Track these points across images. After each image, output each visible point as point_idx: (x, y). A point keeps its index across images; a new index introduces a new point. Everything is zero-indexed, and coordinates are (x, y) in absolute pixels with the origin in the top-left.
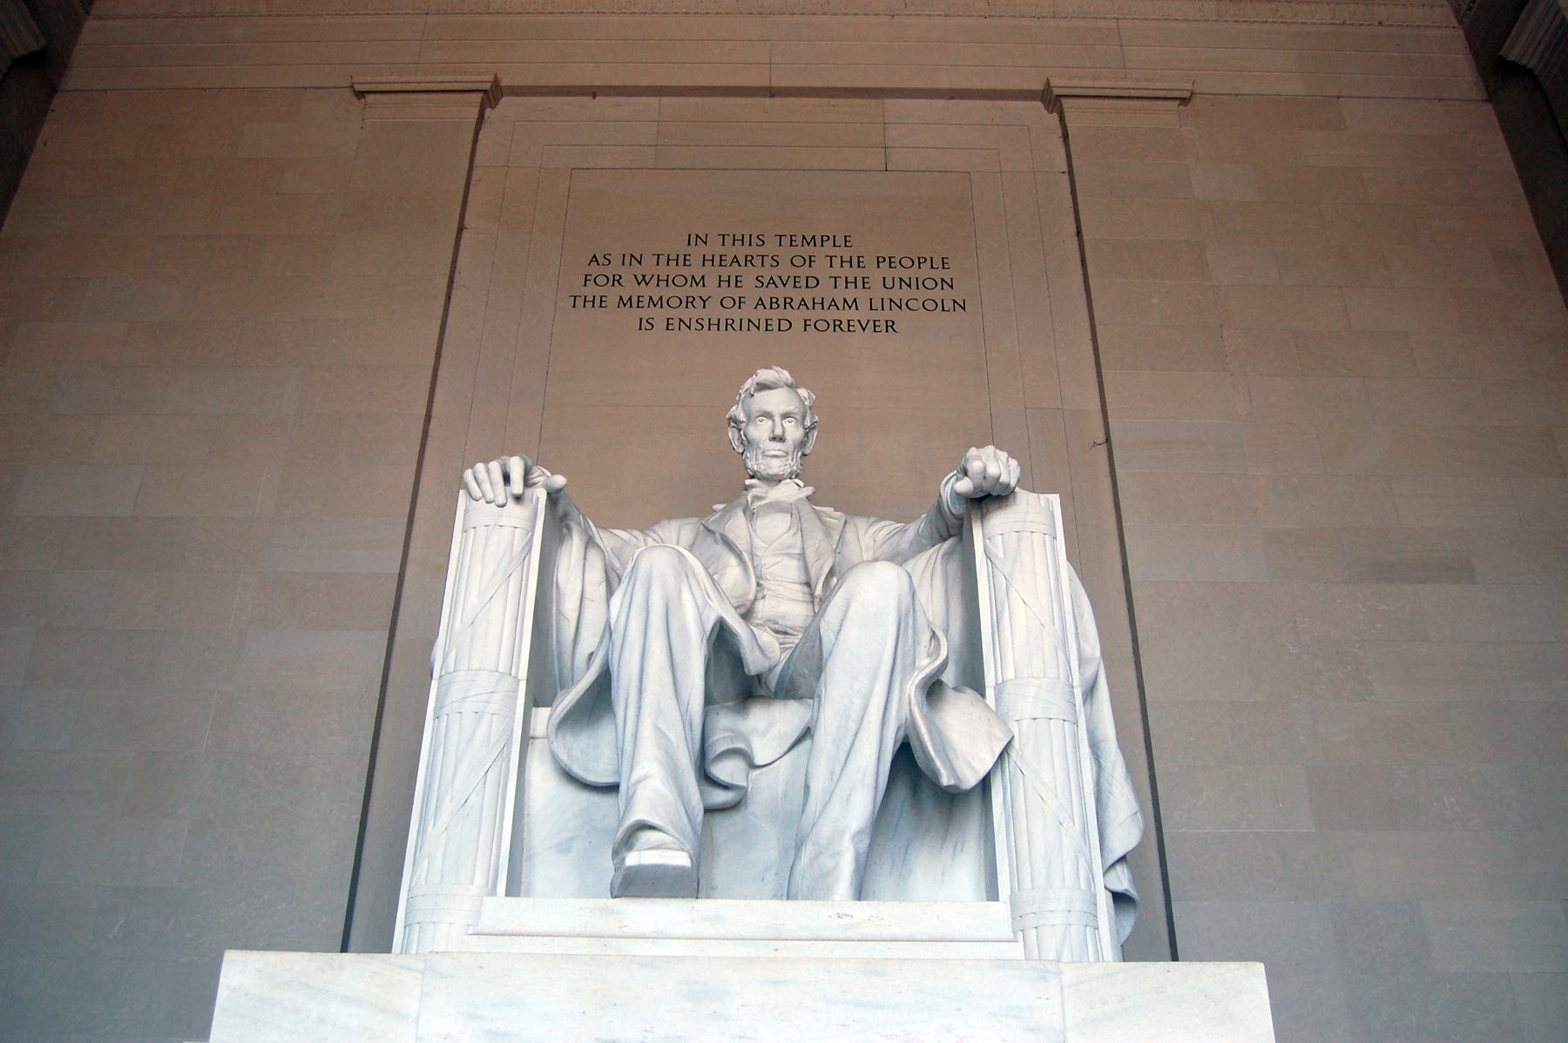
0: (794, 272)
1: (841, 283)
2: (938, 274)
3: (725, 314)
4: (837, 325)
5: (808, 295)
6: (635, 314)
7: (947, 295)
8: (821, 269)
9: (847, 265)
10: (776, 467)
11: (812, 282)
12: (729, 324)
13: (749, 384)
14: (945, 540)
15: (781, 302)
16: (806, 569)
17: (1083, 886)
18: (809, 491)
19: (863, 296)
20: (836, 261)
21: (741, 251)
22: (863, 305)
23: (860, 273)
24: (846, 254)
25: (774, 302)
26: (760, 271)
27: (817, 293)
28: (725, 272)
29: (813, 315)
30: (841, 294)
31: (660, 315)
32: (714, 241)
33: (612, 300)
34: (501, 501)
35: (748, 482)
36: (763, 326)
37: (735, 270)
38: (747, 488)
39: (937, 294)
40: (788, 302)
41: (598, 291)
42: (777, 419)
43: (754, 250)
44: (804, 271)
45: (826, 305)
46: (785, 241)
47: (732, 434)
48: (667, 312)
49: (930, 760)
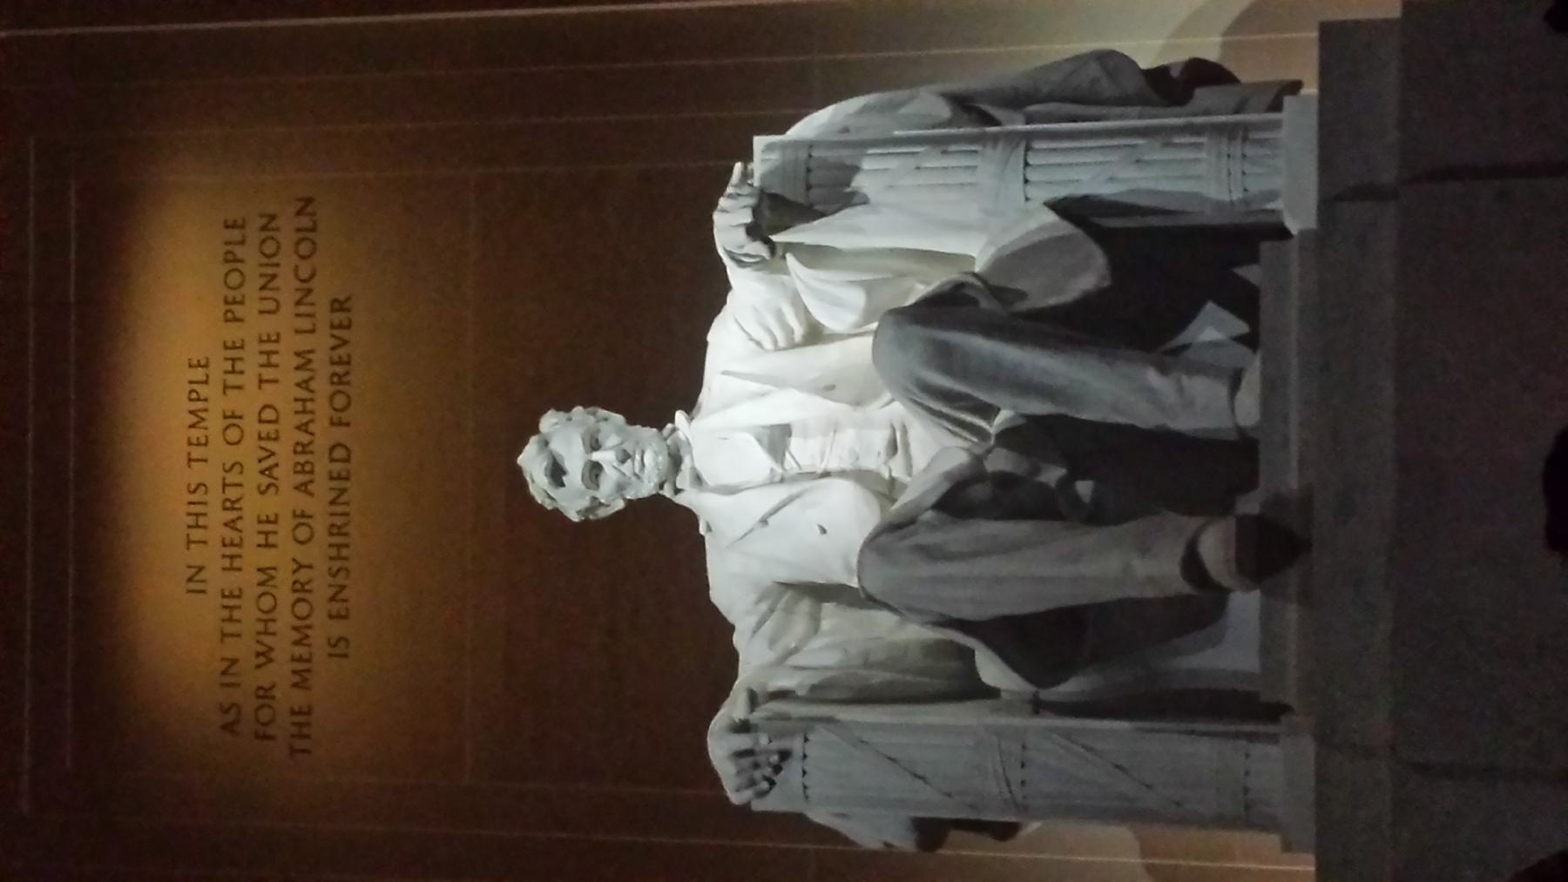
0: (251, 441)
1: (268, 373)
2: (253, 234)
5: (289, 420)
9: (239, 366)
10: (652, 460)
11: (269, 414)
15: (302, 459)
17: (1203, 140)
18: (680, 416)
20: (233, 380)
21: (216, 516)
22: (304, 343)
23: (253, 347)
25: (300, 469)
27: (287, 408)
28: (252, 536)
30: (289, 376)
32: (197, 555)
33: (299, 698)
34: (775, 758)
35: (667, 492)
37: (249, 525)
40: (302, 448)
42: (596, 456)
43: (215, 497)
44: (251, 425)
46: (197, 452)
48: (319, 618)
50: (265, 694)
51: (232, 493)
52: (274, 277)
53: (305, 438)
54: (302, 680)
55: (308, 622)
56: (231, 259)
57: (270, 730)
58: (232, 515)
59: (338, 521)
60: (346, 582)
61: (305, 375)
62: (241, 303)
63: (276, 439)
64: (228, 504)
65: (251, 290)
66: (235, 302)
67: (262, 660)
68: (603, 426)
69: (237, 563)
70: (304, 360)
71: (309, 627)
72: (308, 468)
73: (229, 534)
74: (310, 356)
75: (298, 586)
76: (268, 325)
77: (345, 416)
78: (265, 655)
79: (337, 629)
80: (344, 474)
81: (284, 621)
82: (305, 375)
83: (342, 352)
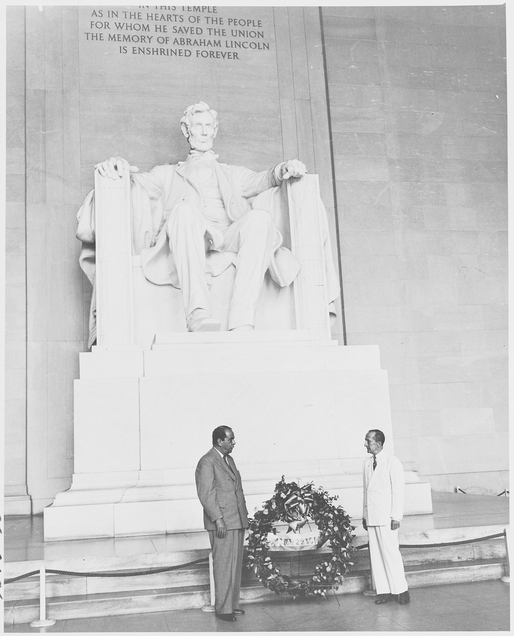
0: (191, 25)
1: (213, 32)
3: (159, 46)
4: (212, 54)
5: (198, 38)
6: (117, 45)
7: (261, 40)
8: (203, 24)
10: (203, 147)
11: (199, 31)
12: (162, 52)
13: (190, 109)
14: (275, 187)
15: (185, 41)
16: (220, 192)
18: (217, 156)
19: (223, 39)
20: (210, 20)
22: (223, 44)
23: (221, 27)
24: (214, 16)
26: (174, 24)
27: (202, 37)
29: (202, 48)
30: (213, 38)
31: (129, 45)
33: (105, 37)
35: (192, 151)
36: (178, 54)
37: (162, 23)
38: (190, 154)
39: (256, 40)
40: (189, 41)
41: (99, 31)
44: (195, 25)
45: (206, 45)
47: (183, 128)
48: (132, 44)
49: (277, 278)
50: (107, 25)
51: (173, 18)
52: (244, 35)
53: (192, 43)
54: (112, 38)
55: (131, 40)
56: (249, 22)
57: (94, 26)
58: (166, 18)
59: (166, 52)
60: (145, 53)
61: (213, 43)
62: (235, 25)
63: (191, 33)
64: (169, 16)
65: (239, 28)
66: (235, 22)
67: (118, 25)
68: (213, 130)
69: (150, 18)
70: (218, 44)
71: (130, 41)
72: (183, 43)
73: (160, 16)
74: (219, 45)
75: (143, 38)
76: (228, 33)
77: (200, 55)
78: (119, 26)
79: (130, 50)
80: (181, 54)
81: (133, 33)
82: (213, 43)
83: (221, 56)
